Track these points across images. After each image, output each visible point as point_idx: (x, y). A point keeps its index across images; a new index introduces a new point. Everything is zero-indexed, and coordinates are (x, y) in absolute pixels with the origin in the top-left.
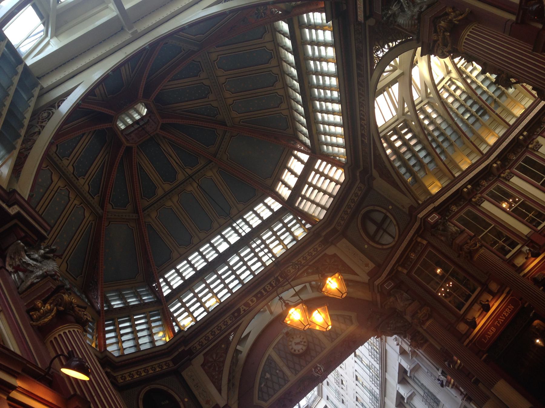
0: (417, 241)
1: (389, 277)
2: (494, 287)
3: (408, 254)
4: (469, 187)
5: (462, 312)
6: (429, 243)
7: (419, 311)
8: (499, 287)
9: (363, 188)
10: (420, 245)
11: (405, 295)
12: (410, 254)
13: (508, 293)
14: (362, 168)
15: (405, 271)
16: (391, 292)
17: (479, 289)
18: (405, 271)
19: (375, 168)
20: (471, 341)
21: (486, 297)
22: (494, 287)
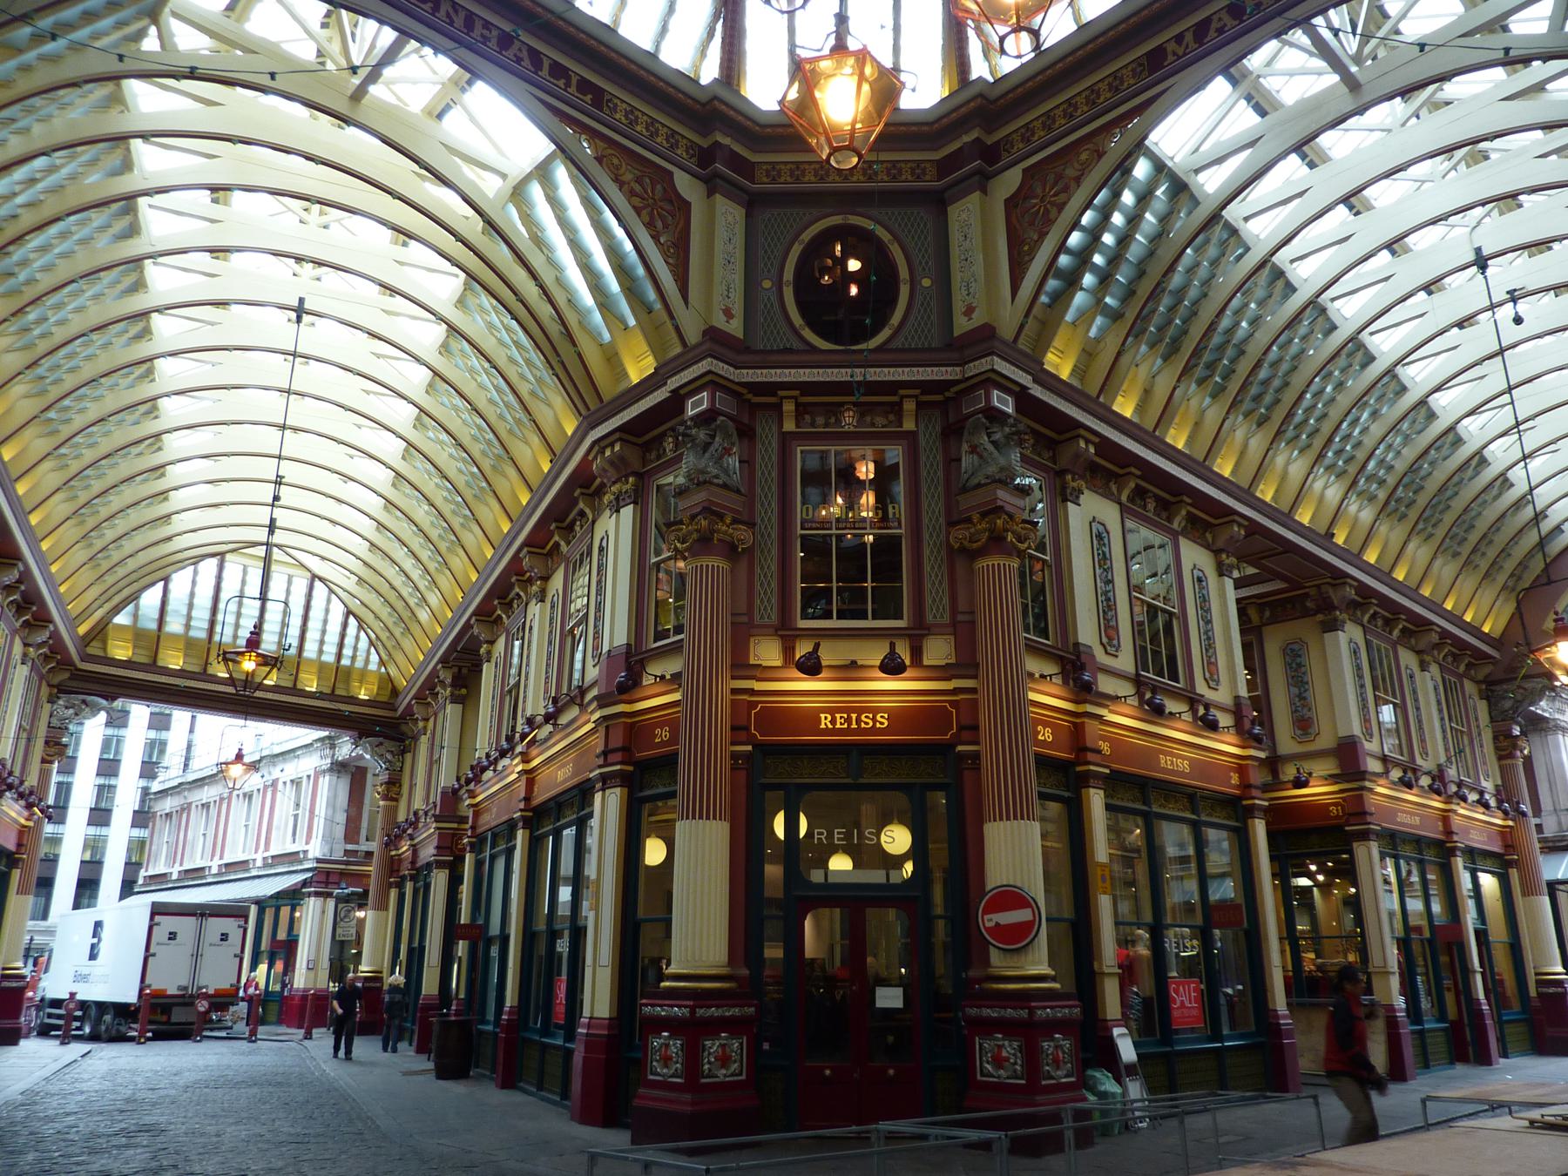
0: (900, 404)
1: (744, 391)
2: (938, 651)
3: (842, 404)
4: (1092, 450)
8: (953, 661)
9: (928, 178)
10: (891, 417)
11: (733, 462)
12: (849, 409)
13: (955, 691)
14: (990, 140)
15: (789, 426)
16: (722, 418)
19: (1025, 171)
20: (752, 692)
22: (938, 651)
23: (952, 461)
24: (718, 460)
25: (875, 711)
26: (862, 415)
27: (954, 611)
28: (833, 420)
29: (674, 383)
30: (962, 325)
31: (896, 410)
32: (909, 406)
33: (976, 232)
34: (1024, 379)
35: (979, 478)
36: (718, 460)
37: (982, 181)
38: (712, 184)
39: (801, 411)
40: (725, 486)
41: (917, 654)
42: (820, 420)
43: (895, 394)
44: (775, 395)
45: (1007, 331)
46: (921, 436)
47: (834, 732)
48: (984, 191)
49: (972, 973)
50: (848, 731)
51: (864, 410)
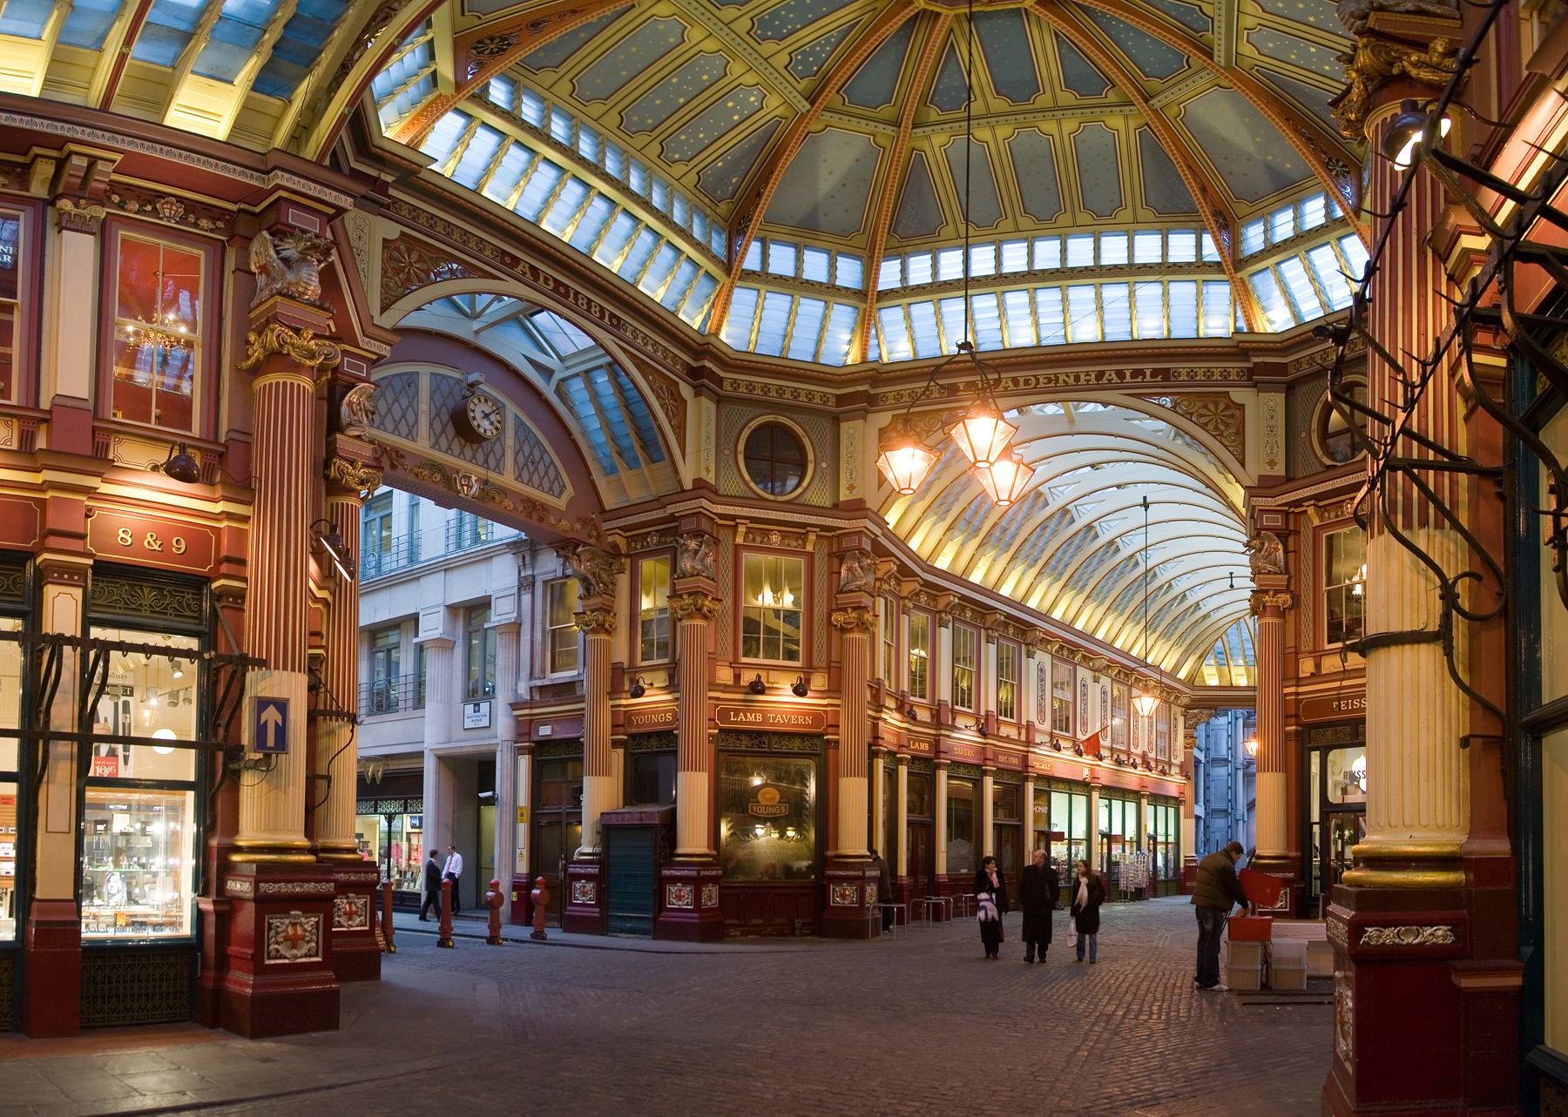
3: (772, 530)
6: (812, 554)
7: (710, 598)
10: (800, 542)
11: (709, 560)
15: (740, 540)
24: (702, 561)
26: (782, 539)
28: (766, 539)
30: (844, 496)
31: (803, 538)
32: (812, 537)
34: (878, 531)
36: (702, 561)
40: (708, 578)
42: (758, 539)
43: (804, 528)
44: (734, 520)
45: (872, 504)
46: (816, 558)
51: (784, 535)
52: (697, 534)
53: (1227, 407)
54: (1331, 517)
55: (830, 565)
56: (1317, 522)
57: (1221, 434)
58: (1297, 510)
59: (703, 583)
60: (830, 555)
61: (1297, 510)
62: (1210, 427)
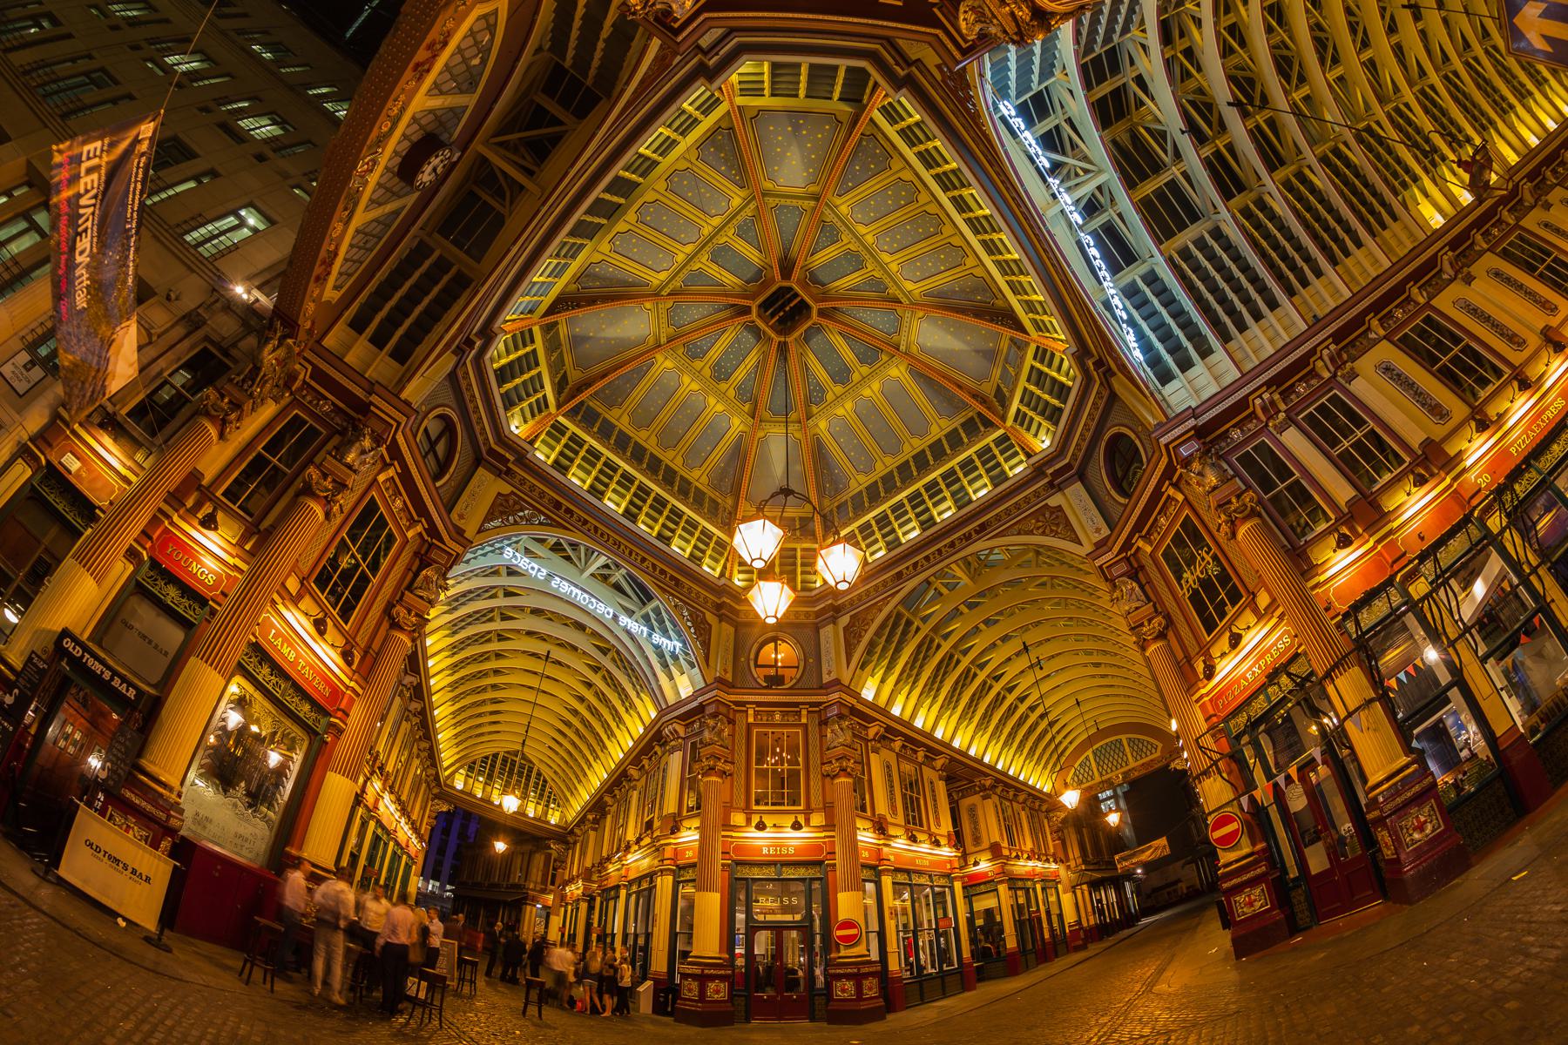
2: (818, 819)
5: (755, 808)
15: (751, 720)
17: (801, 808)
18: (751, 720)
21: (801, 819)
22: (818, 819)
23: (823, 736)
25: (788, 846)
27: (824, 803)
29: (700, 699)
30: (826, 679)
32: (804, 712)
33: (831, 640)
34: (854, 702)
35: (835, 744)
37: (834, 620)
38: (721, 618)
39: (756, 713)
41: (807, 821)
47: (769, 855)
48: (834, 623)
49: (833, 955)
50: (776, 855)
51: (784, 714)
52: (714, 716)
53: (1052, 513)
54: (1156, 537)
55: (820, 731)
56: (1149, 549)
57: (1057, 533)
58: (1133, 551)
59: (717, 749)
60: (820, 724)
61: (1133, 551)
62: (1047, 531)
